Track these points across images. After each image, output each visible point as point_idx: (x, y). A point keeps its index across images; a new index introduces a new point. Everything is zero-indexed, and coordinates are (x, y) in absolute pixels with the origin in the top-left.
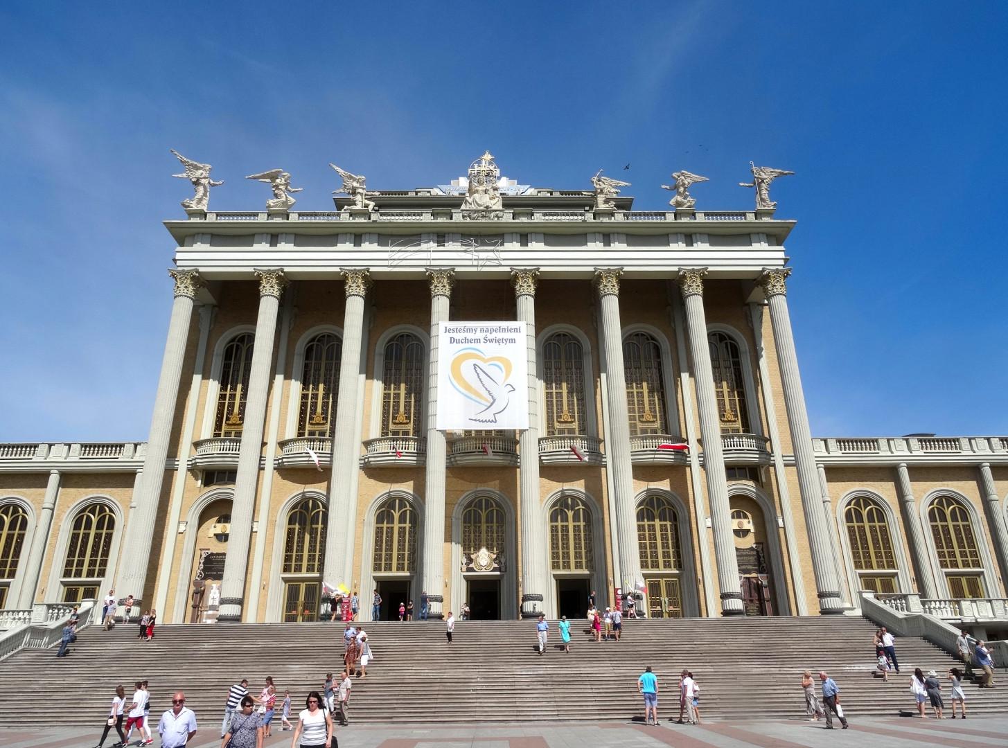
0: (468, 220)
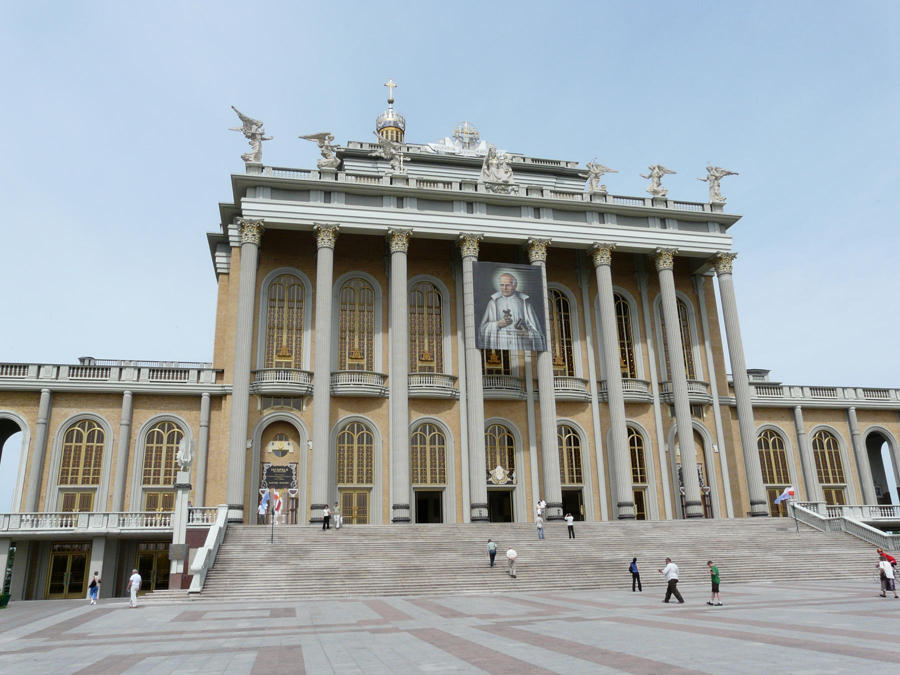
0: (491, 193)
